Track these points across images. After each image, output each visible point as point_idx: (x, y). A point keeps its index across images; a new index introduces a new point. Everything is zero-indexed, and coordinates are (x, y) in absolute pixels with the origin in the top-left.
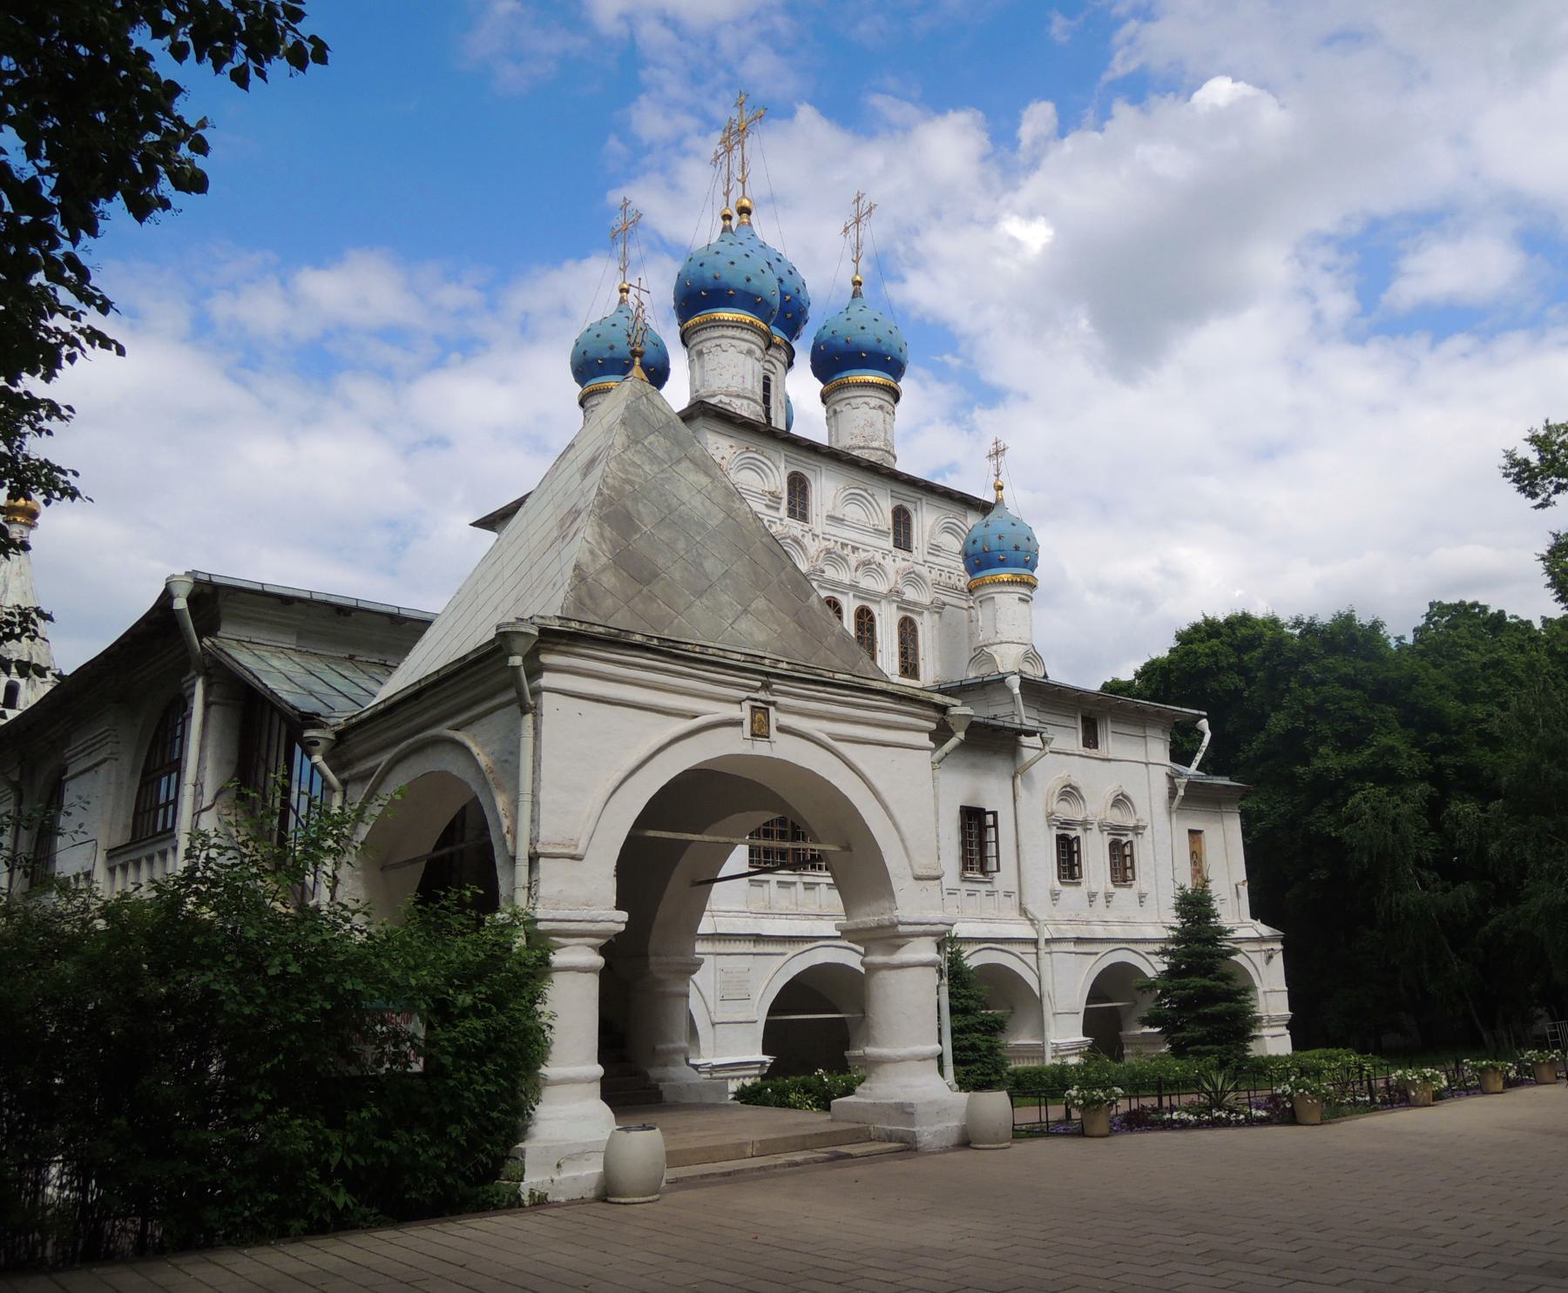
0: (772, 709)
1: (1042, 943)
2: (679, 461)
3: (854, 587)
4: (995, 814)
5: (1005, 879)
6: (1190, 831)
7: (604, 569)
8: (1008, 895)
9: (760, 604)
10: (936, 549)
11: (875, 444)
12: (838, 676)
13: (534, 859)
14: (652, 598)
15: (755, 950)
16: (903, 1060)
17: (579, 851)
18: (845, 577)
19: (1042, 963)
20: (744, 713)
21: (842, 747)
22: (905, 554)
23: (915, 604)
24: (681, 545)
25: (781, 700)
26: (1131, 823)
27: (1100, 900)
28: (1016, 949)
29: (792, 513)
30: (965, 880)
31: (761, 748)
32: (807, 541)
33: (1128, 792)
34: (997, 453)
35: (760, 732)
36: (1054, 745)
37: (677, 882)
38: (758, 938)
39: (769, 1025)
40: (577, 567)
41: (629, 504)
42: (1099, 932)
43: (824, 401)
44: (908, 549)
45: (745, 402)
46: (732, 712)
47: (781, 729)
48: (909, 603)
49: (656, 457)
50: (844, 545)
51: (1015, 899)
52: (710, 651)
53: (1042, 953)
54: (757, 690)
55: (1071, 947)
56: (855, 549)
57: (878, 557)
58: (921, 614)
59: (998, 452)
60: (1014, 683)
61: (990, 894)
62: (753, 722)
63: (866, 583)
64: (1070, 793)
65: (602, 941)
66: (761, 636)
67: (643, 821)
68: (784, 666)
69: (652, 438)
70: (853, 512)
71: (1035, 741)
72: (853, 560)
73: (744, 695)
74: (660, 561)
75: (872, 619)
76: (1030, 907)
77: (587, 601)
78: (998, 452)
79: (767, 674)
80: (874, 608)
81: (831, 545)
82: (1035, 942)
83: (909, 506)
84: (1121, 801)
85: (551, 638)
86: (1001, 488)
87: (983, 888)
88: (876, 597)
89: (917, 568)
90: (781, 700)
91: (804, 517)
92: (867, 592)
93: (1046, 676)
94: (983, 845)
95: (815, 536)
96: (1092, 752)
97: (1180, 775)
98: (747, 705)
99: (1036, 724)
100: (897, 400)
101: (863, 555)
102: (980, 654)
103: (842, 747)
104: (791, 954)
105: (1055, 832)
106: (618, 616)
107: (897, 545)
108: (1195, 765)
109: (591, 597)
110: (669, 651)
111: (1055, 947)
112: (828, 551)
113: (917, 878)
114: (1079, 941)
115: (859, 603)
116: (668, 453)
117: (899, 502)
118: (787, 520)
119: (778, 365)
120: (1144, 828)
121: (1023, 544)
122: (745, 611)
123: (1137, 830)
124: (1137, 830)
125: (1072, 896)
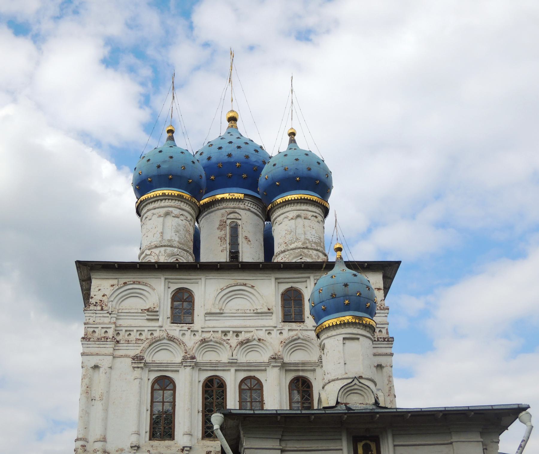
11: (293, 246)
18: (224, 357)
22: (294, 325)
23: (304, 364)
29: (176, 319)
45: (162, 249)
50: (225, 333)
57: (262, 334)
58: (314, 370)
63: (242, 358)
81: (206, 335)
88: (262, 367)
92: (249, 364)
93: (376, 403)
95: (194, 333)
107: (287, 319)
115: (242, 375)
117: (288, 286)
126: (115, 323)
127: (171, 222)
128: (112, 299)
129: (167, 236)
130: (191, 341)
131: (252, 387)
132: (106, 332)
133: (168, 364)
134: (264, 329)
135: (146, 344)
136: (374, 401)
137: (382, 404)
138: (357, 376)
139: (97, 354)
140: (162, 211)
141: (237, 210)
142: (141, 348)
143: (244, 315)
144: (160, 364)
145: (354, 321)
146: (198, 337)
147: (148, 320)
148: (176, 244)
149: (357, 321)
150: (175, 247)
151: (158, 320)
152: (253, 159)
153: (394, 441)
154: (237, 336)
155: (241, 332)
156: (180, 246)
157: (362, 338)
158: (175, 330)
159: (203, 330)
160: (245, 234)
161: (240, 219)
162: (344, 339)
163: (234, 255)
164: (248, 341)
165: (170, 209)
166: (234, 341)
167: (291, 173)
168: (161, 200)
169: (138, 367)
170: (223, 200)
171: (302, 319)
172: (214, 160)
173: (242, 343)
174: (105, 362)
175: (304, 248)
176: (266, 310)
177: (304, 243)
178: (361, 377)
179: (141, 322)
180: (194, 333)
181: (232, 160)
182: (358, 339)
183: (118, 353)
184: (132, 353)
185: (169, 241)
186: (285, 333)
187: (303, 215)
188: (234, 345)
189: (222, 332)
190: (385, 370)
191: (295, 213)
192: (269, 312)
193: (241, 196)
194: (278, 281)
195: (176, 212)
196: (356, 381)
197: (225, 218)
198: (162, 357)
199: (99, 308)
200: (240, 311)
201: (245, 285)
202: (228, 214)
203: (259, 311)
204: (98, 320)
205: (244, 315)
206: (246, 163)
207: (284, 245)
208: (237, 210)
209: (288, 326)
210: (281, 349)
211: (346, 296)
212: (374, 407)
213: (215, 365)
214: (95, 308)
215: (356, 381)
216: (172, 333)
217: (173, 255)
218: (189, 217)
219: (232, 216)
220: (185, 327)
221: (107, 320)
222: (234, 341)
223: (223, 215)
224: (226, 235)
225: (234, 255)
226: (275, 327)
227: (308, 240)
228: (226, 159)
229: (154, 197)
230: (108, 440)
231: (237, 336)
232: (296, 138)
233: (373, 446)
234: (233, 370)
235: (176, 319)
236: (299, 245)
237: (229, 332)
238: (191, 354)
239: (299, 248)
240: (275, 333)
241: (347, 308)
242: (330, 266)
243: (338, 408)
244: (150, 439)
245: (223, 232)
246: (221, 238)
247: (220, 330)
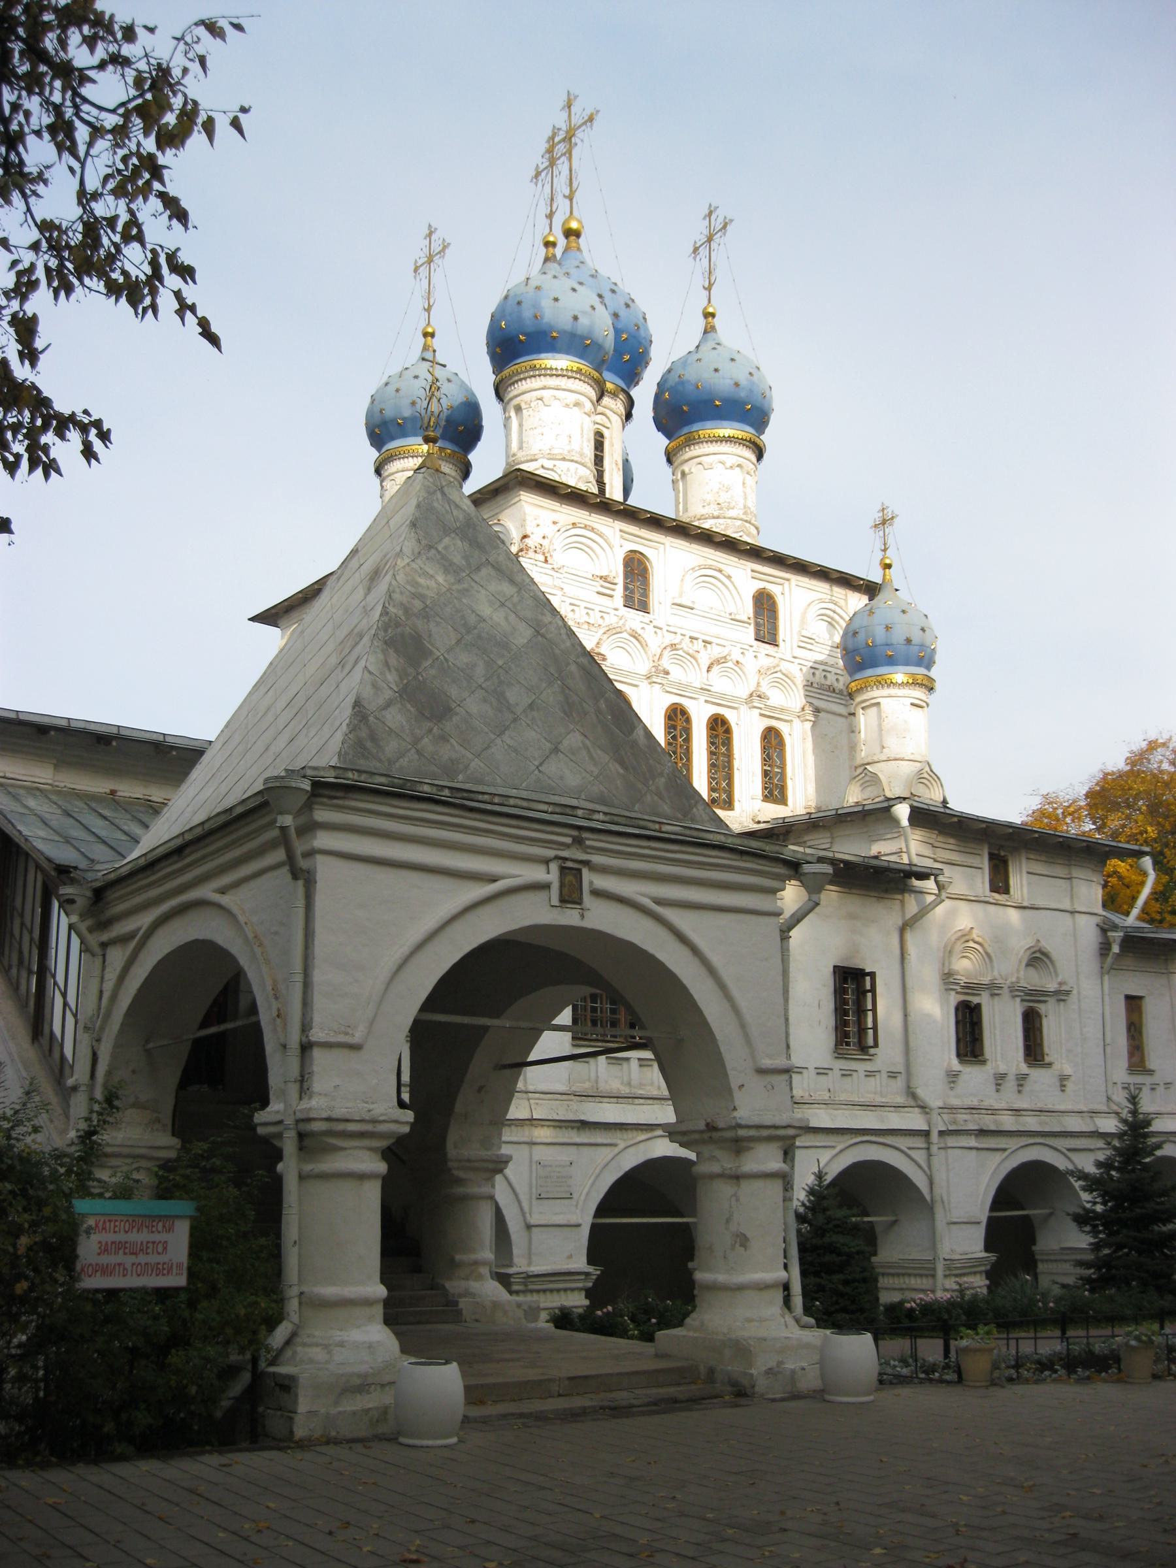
0: (585, 872)
1: (934, 1136)
2: (478, 569)
4: (872, 975)
5: (888, 1053)
6: (1128, 998)
7: (388, 704)
8: (893, 1075)
9: (573, 740)
10: (807, 641)
11: (731, 513)
12: (665, 828)
13: (306, 1048)
14: (444, 738)
15: (578, 1140)
16: (741, 1288)
17: (357, 1039)
19: (935, 1161)
20: (552, 875)
21: (669, 914)
23: (782, 710)
24: (480, 670)
25: (597, 859)
26: (1052, 986)
27: (1010, 1084)
28: (903, 1142)
29: (629, 602)
31: (570, 917)
32: (648, 634)
33: (1047, 945)
34: (884, 522)
35: (571, 896)
36: (952, 890)
37: (480, 1064)
38: (584, 1125)
39: (596, 1231)
40: (357, 704)
41: (420, 624)
42: (1008, 1122)
43: (669, 461)
44: (773, 642)
46: (537, 874)
47: (597, 893)
48: (773, 708)
49: (452, 564)
51: (900, 1082)
52: (512, 802)
53: (934, 1149)
54: (567, 846)
55: (972, 1142)
57: (736, 655)
59: (884, 522)
60: (902, 811)
61: (870, 1074)
62: (562, 885)
65: (384, 1143)
66: (573, 779)
67: (430, 1004)
68: (601, 817)
69: (446, 541)
70: (705, 598)
71: (930, 885)
72: (705, 658)
73: (551, 853)
74: (454, 692)
75: (728, 731)
76: (920, 1092)
77: (369, 744)
78: (884, 522)
79: (579, 828)
80: (730, 716)
81: (677, 639)
82: (926, 1134)
83: (774, 589)
84: (1038, 958)
85: (324, 789)
86: (889, 566)
89: (784, 666)
90: (597, 859)
91: (644, 607)
92: (723, 696)
93: (945, 802)
94: (861, 1012)
97: (1115, 927)
98: (554, 867)
99: (929, 863)
100: (760, 457)
101: (716, 652)
102: (864, 774)
103: (669, 914)
104: (622, 1145)
105: (954, 999)
106: (404, 762)
108: (1135, 912)
109: (373, 737)
110: (464, 803)
111: (951, 1141)
112: (673, 647)
113: (762, 1071)
114: (982, 1133)
116: (466, 558)
117: (762, 585)
118: (625, 611)
120: (1068, 993)
121: (916, 637)
122: (556, 750)
123: (1061, 995)
125: (975, 1078)
134: (740, 646)
158: (634, 618)
159: (670, 629)
167: (743, 394)
171: (775, 640)
186: (761, 656)
199: (542, 559)
200: (713, 611)
201: (720, 571)
203: (738, 617)
206: (635, 337)
213: (682, 688)
215: (927, 769)
232: (717, 322)
234: (703, 698)
237: (696, 639)
247: (689, 634)
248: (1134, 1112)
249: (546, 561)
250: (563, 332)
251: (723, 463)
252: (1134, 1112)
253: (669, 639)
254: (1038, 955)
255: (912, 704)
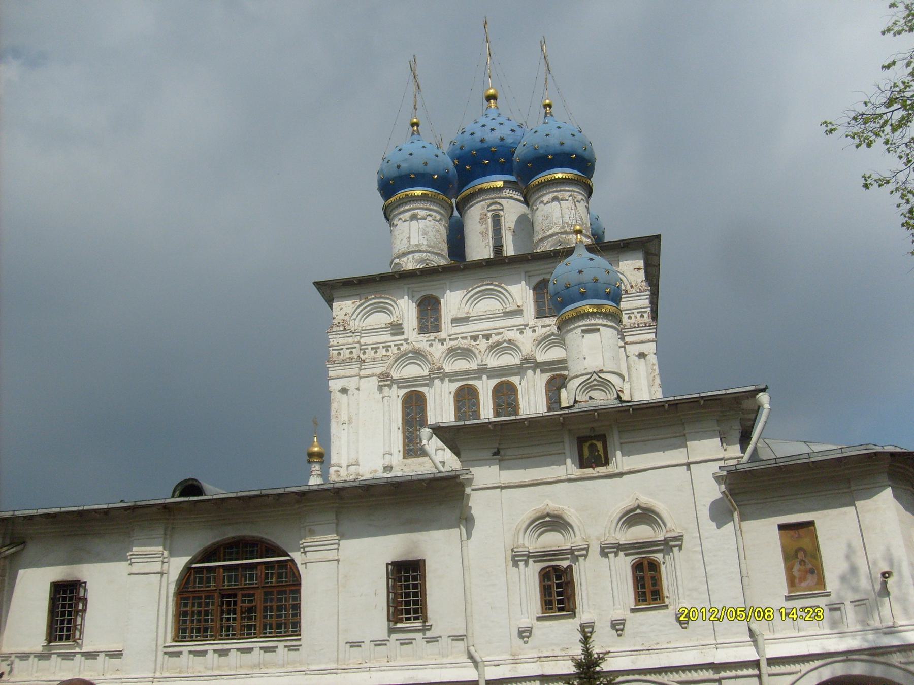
3: (483, 371)
11: (551, 232)
26: (661, 537)
29: (423, 329)
30: (391, 631)
45: (410, 256)
50: (475, 338)
56: (487, 337)
57: (512, 335)
63: (493, 362)
64: (554, 522)
80: (515, 380)
87: (419, 636)
93: (619, 397)
95: (442, 341)
96: (602, 470)
101: (495, 339)
115: (494, 382)
119: (503, 201)
124: (669, 545)
126: (359, 342)
127: (429, 223)
128: (354, 317)
129: (414, 241)
130: (438, 351)
131: (505, 395)
132: (351, 352)
133: (416, 379)
134: (515, 328)
135: (392, 360)
136: (616, 396)
137: (625, 397)
138: (596, 370)
139: (343, 377)
140: (407, 215)
141: (498, 200)
142: (387, 365)
143: (492, 317)
144: (407, 380)
145: (591, 310)
146: (446, 346)
147: (393, 335)
148: (424, 248)
149: (595, 310)
150: (424, 252)
151: (403, 333)
152: (509, 140)
153: (620, 438)
154: (488, 339)
155: (490, 335)
156: (430, 249)
157: (602, 328)
158: (420, 341)
160: (507, 226)
161: (502, 210)
162: (583, 331)
163: (498, 248)
164: (498, 344)
165: (416, 211)
166: (483, 344)
167: (541, 151)
168: (406, 203)
169: (385, 385)
170: (482, 191)
172: (466, 148)
173: (491, 347)
174: (351, 383)
175: (562, 233)
176: (515, 308)
177: (563, 227)
178: (601, 371)
179: (387, 337)
180: (442, 341)
181: (485, 145)
182: (598, 330)
183: (362, 373)
184: (378, 371)
185: (416, 245)
187: (560, 197)
188: (483, 350)
189: (472, 337)
190: (648, 357)
191: (551, 196)
192: (519, 312)
193: (500, 184)
194: (528, 276)
195: (422, 213)
196: (595, 376)
197: (485, 210)
198: (412, 371)
199: (342, 328)
201: (491, 284)
202: (489, 206)
204: (341, 341)
205: (492, 317)
207: (541, 233)
208: (498, 200)
209: (541, 322)
210: (534, 348)
211: (580, 284)
212: (617, 402)
214: (338, 329)
215: (595, 376)
216: (418, 346)
217: (422, 261)
218: (438, 217)
219: (493, 207)
220: (432, 336)
221: (350, 340)
222: (483, 344)
223: (483, 208)
224: (487, 229)
225: (498, 248)
226: (527, 325)
227: (567, 223)
228: (479, 145)
229: (397, 201)
230: (361, 464)
231: (488, 339)
233: (599, 445)
234: (485, 377)
235: (423, 329)
236: (556, 229)
237: (478, 336)
238: (439, 365)
239: (557, 234)
240: (528, 332)
241: (583, 296)
242: (569, 252)
243: (577, 405)
244: (404, 458)
245: (484, 226)
246: (482, 233)
248: (587, 652)
249: (345, 329)
250: (394, 179)
251: (542, 202)
252: (587, 652)
253: (449, 344)
254: (638, 511)
255: (584, 331)
